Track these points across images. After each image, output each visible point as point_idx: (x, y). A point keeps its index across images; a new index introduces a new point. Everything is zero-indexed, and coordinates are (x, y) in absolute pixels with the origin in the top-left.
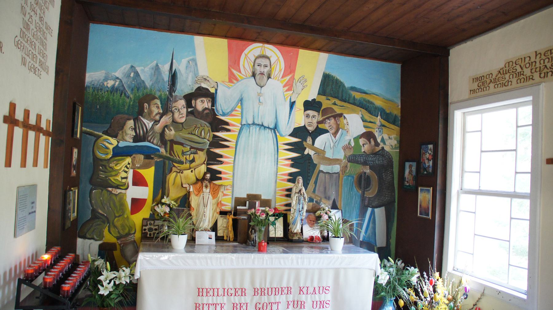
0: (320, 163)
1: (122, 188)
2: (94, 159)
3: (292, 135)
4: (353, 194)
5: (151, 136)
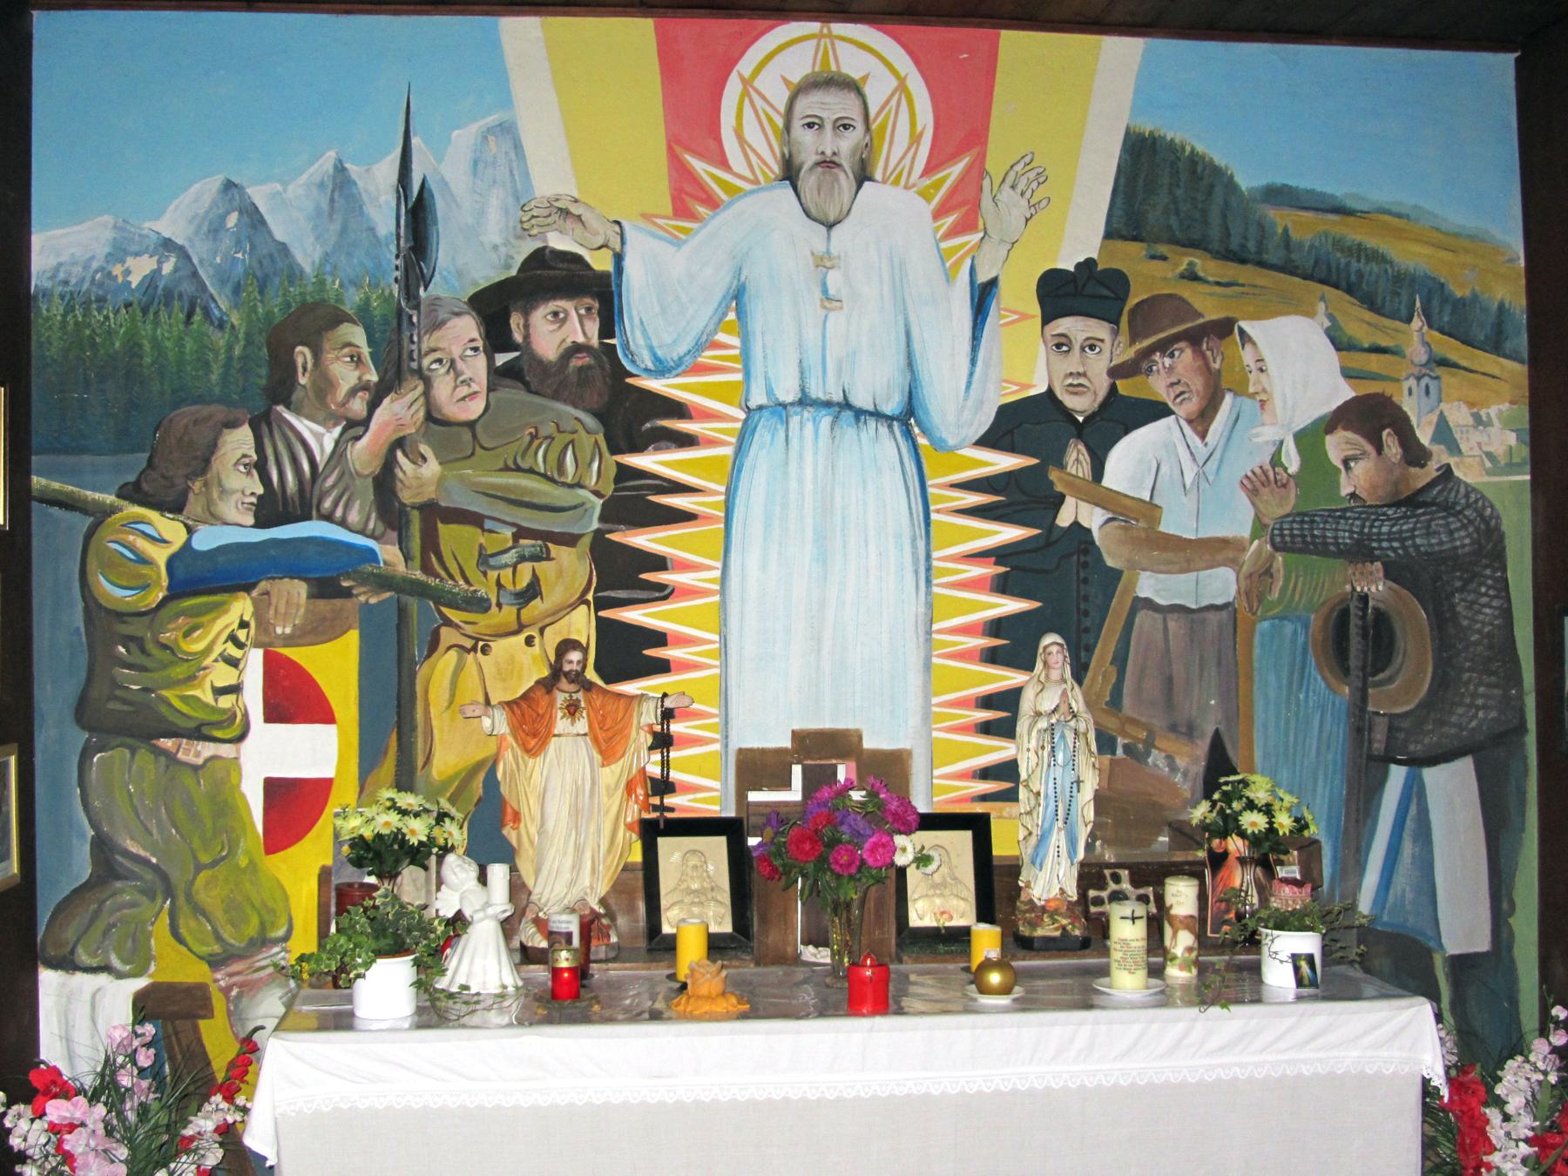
0: (1135, 567)
1: (218, 734)
2: (87, 611)
3: (991, 440)
4: (1311, 704)
5: (335, 493)
